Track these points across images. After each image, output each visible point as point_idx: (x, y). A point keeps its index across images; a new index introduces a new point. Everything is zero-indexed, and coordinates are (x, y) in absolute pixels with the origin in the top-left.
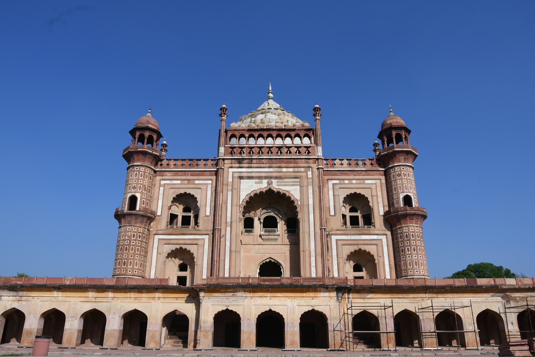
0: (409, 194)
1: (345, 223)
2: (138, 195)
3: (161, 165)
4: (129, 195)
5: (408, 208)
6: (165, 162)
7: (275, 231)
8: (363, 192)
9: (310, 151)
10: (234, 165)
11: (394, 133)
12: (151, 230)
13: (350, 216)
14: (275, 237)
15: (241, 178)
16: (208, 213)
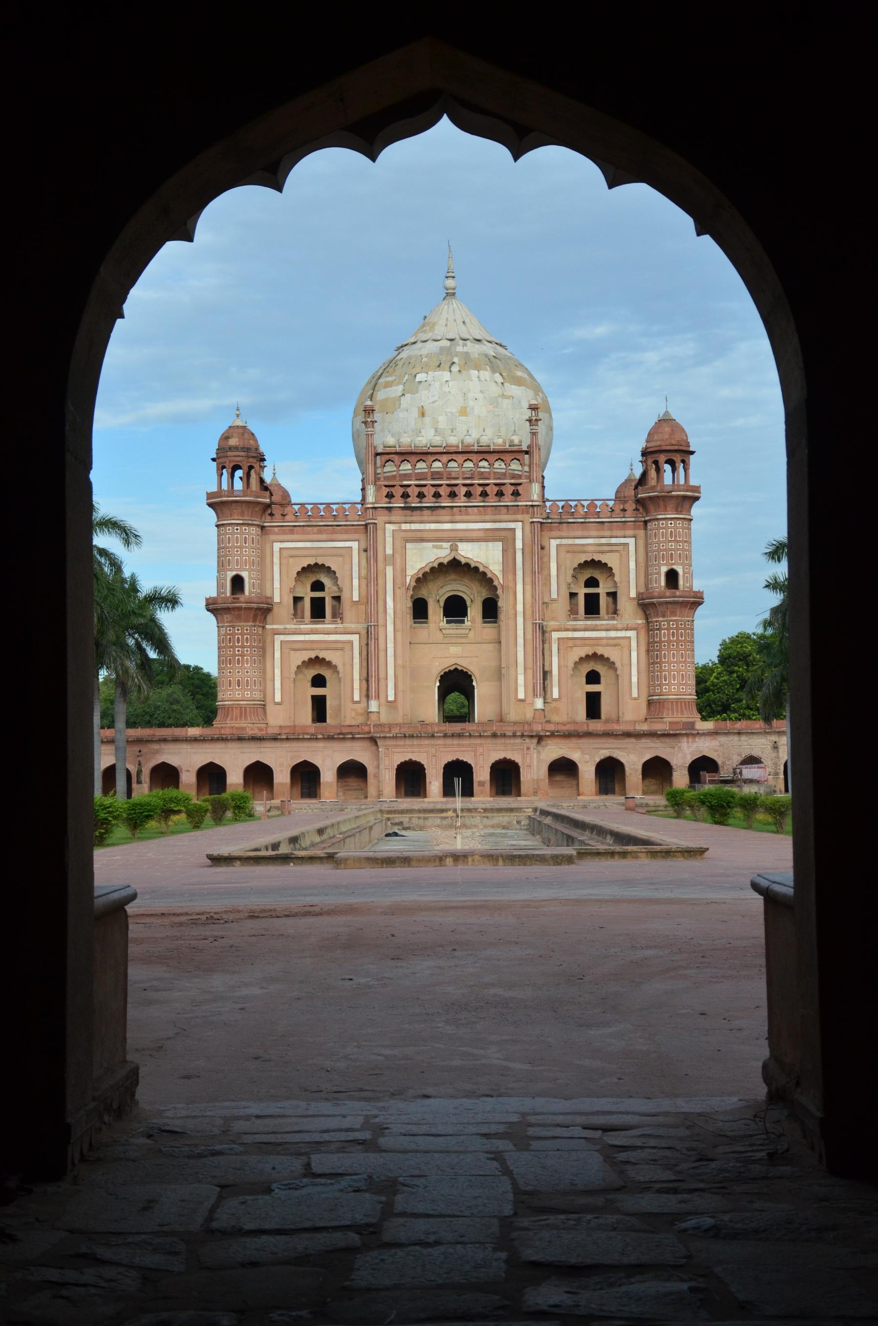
0: (675, 567)
1: (573, 611)
2: (245, 574)
3: (271, 515)
4: (230, 574)
5: (668, 592)
6: (276, 510)
7: (463, 622)
8: (604, 559)
9: (520, 492)
10: (393, 518)
11: (662, 458)
12: (268, 627)
13: (586, 595)
14: (463, 631)
15: (407, 541)
16: (356, 598)
